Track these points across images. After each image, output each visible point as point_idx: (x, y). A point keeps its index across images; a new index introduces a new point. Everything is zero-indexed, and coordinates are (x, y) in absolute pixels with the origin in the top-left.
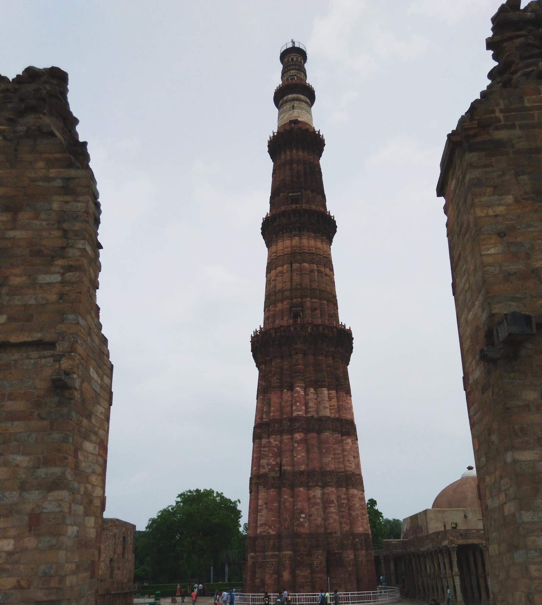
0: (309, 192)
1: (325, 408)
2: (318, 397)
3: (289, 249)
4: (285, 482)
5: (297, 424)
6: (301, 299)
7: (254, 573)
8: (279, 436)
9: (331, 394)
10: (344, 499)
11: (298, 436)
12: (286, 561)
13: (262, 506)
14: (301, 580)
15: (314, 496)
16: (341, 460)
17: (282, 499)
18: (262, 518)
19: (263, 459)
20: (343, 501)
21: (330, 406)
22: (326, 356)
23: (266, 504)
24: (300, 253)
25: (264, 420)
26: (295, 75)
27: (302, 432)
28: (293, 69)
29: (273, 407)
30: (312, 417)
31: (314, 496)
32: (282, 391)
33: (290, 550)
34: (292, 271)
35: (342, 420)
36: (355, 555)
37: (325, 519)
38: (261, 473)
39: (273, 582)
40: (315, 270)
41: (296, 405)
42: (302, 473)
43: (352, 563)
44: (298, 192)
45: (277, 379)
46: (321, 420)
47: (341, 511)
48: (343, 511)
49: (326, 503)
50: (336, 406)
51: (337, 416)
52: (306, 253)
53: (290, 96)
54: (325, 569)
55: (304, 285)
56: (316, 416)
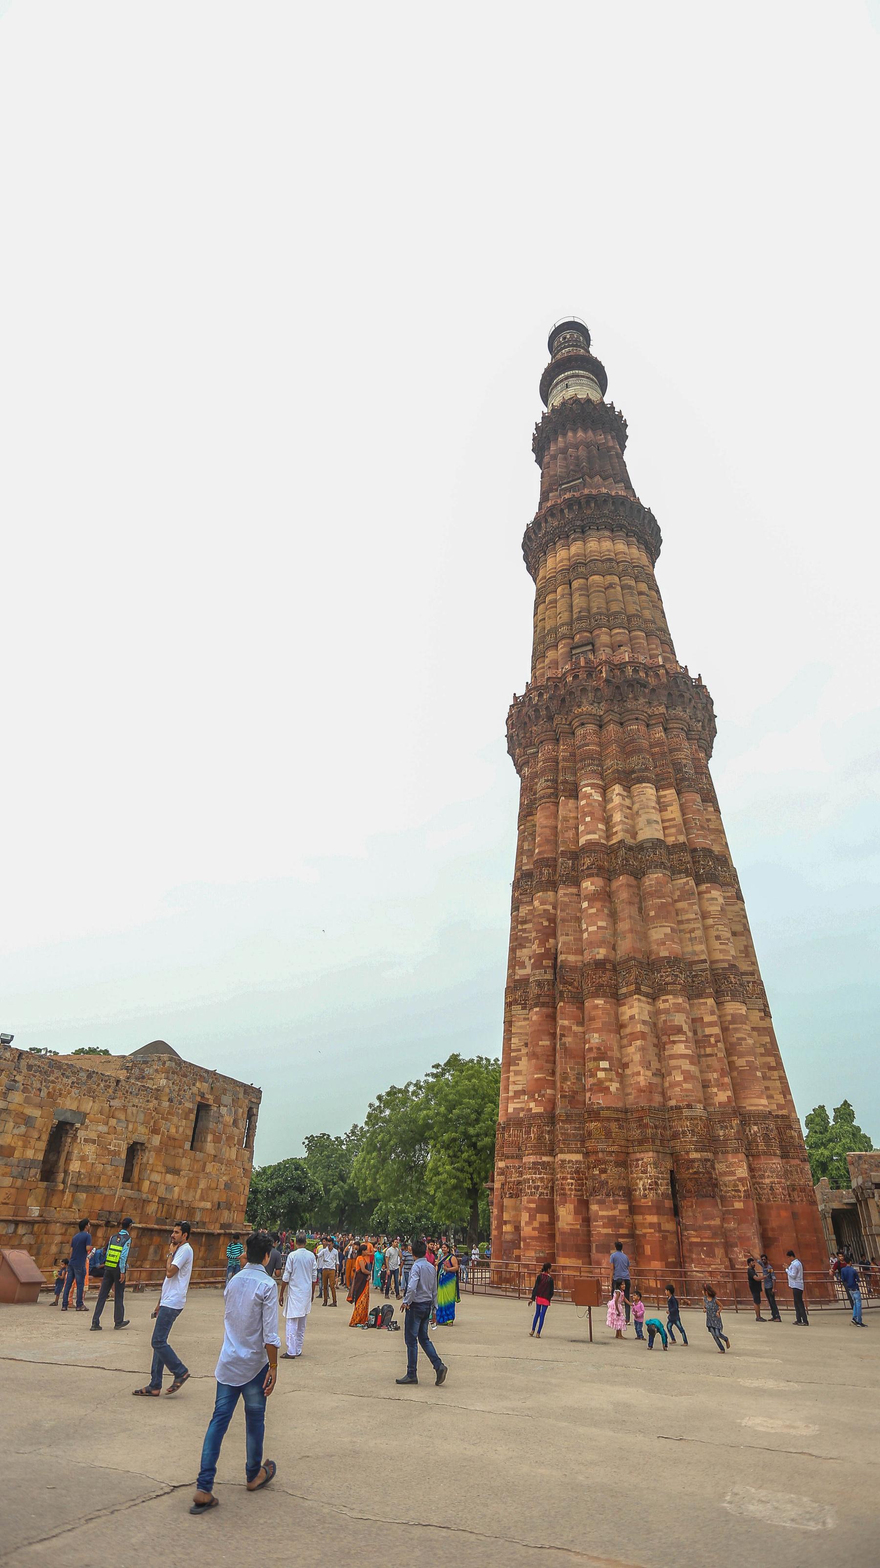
1: (649, 822)
3: (566, 562)
6: (591, 633)
7: (501, 1209)
8: (550, 893)
9: (665, 796)
10: (711, 1024)
12: (564, 1178)
13: (520, 1050)
14: (604, 1231)
16: (698, 933)
18: (519, 1078)
19: (522, 946)
20: (708, 1031)
21: (663, 821)
23: (526, 1045)
27: (598, 875)
31: (632, 1017)
32: (557, 804)
33: (577, 1152)
36: (751, 1169)
37: (660, 1074)
38: (517, 977)
42: (600, 965)
44: (579, 479)
46: (640, 847)
48: (711, 1055)
50: (679, 820)
54: (668, 1204)
56: (630, 841)
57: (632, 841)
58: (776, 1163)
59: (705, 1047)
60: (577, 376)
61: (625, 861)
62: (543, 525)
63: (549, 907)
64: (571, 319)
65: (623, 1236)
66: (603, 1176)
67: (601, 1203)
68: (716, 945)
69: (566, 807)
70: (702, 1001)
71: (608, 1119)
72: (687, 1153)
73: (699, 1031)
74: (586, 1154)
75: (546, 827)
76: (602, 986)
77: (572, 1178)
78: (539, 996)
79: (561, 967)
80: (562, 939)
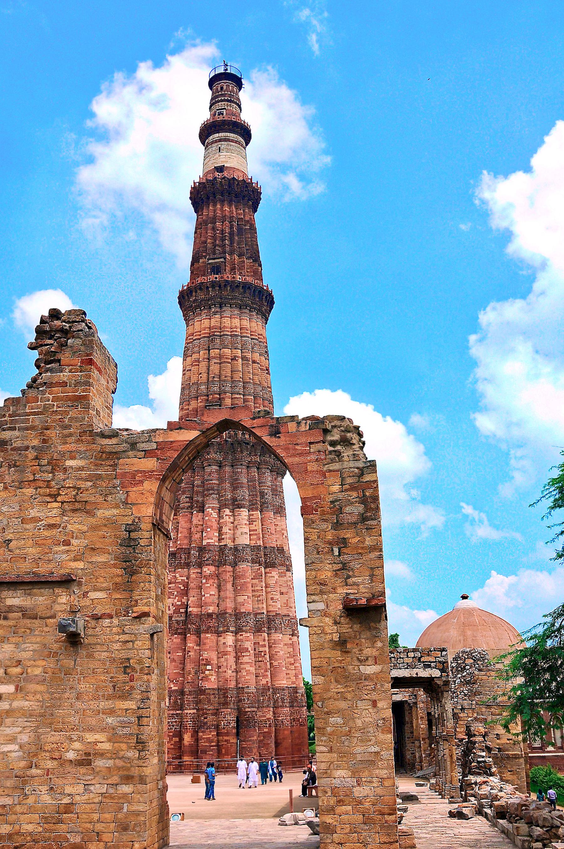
6: (219, 394)
9: (253, 515)
11: (208, 570)
15: (224, 643)
20: (261, 649)
22: (248, 467)
24: (221, 336)
26: (225, 109)
27: (212, 565)
28: (222, 101)
30: (225, 545)
31: (224, 643)
35: (265, 547)
40: (238, 357)
42: (210, 615)
45: (187, 497)
48: (261, 661)
49: (239, 651)
52: (227, 335)
54: (234, 731)
56: (230, 544)
57: (232, 544)
58: (286, 710)
59: (259, 657)
60: (229, 140)
61: (227, 557)
62: (194, 294)
65: (213, 746)
68: (271, 602)
69: (197, 518)
71: (209, 694)
72: (245, 709)
73: (257, 650)
74: (198, 710)
75: (185, 528)
77: (191, 721)
79: (190, 615)
80: (191, 599)
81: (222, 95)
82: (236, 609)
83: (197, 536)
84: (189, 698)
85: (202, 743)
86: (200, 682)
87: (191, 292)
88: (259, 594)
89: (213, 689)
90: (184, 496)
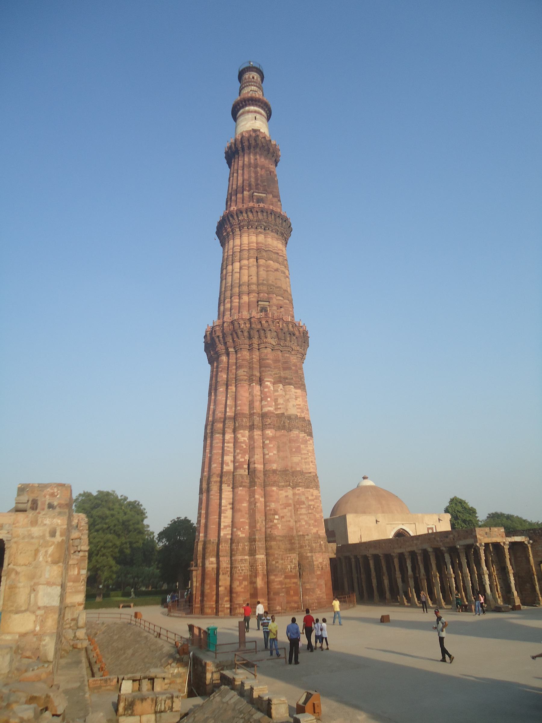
0: (271, 196)
2: (286, 394)
4: (256, 480)
5: (268, 419)
10: (313, 500)
17: (253, 499)
18: (226, 520)
20: (310, 503)
23: (230, 504)
24: (266, 251)
25: (228, 414)
28: (254, 86)
29: (240, 400)
30: (283, 414)
31: (287, 496)
34: (258, 267)
39: (243, 590)
41: (266, 400)
42: (274, 471)
43: (320, 566)
46: (289, 418)
47: (309, 513)
51: (303, 415)
53: (252, 108)
55: (270, 282)
56: (286, 414)
60: (261, 114)
63: (246, 439)
64: (258, 66)
65: (283, 588)
66: (277, 565)
67: (276, 575)
70: (308, 490)
71: (280, 541)
72: (307, 553)
74: (267, 555)
76: (275, 481)
78: (242, 482)
80: (256, 456)
81: (254, 82)
82: (292, 468)
83: (257, 404)
84: (260, 544)
85: (276, 586)
86: (269, 530)
87: (241, 213)
88: (305, 456)
89: (281, 536)
90: (242, 370)
